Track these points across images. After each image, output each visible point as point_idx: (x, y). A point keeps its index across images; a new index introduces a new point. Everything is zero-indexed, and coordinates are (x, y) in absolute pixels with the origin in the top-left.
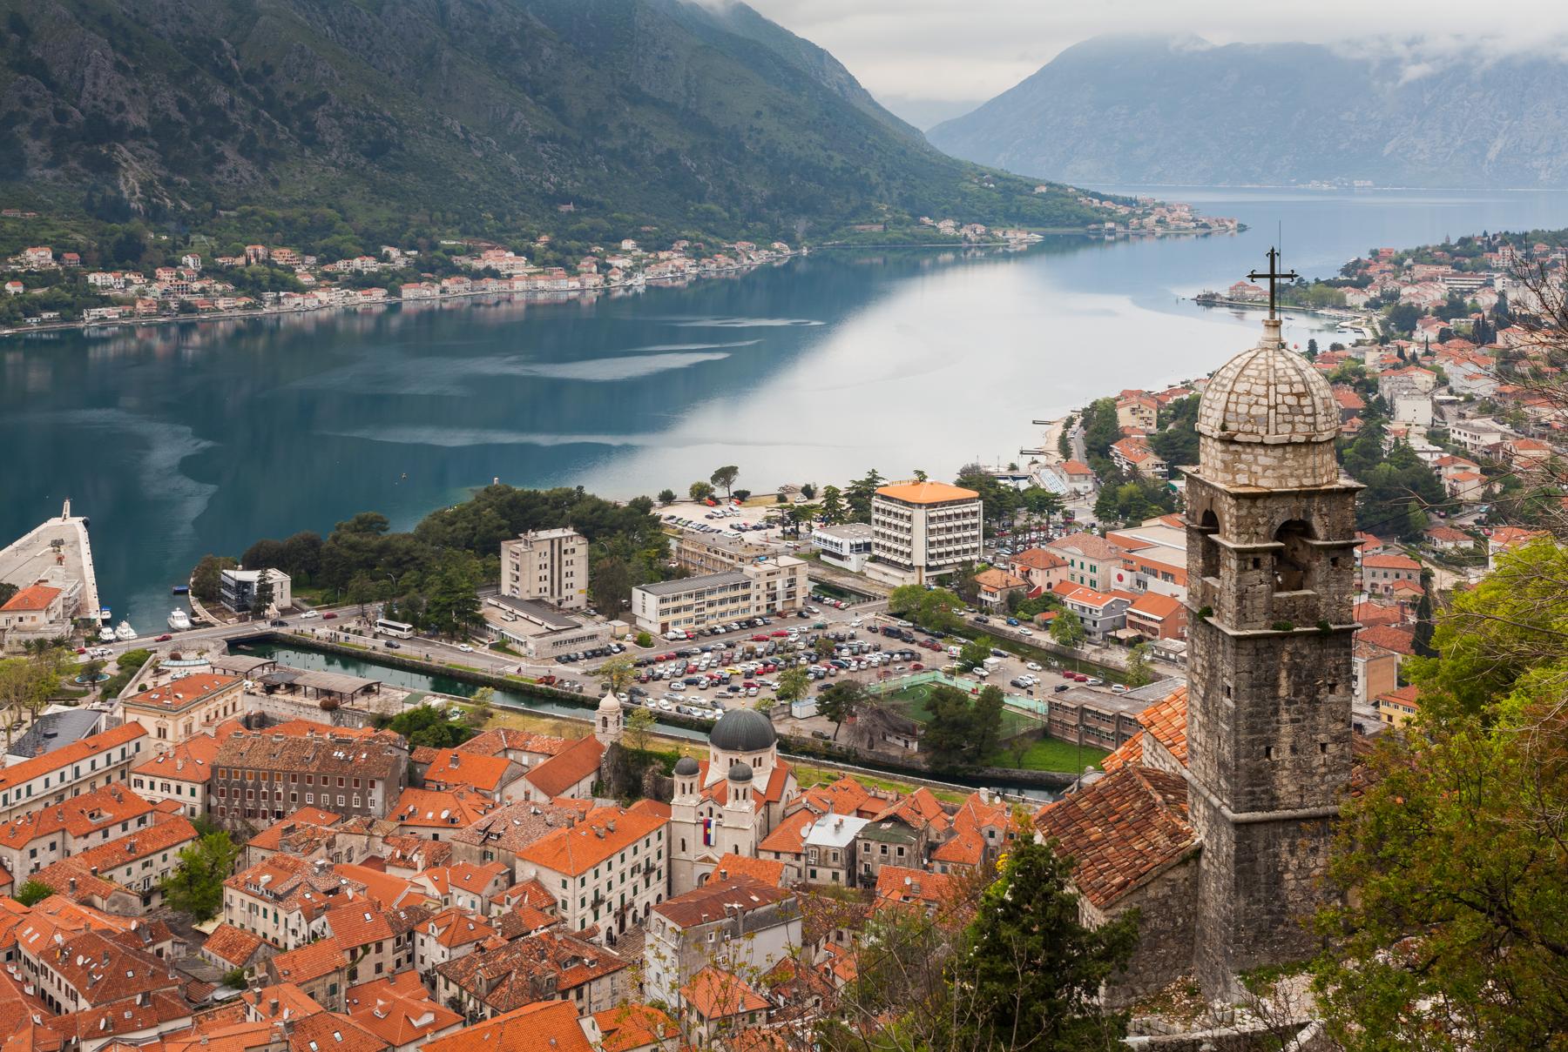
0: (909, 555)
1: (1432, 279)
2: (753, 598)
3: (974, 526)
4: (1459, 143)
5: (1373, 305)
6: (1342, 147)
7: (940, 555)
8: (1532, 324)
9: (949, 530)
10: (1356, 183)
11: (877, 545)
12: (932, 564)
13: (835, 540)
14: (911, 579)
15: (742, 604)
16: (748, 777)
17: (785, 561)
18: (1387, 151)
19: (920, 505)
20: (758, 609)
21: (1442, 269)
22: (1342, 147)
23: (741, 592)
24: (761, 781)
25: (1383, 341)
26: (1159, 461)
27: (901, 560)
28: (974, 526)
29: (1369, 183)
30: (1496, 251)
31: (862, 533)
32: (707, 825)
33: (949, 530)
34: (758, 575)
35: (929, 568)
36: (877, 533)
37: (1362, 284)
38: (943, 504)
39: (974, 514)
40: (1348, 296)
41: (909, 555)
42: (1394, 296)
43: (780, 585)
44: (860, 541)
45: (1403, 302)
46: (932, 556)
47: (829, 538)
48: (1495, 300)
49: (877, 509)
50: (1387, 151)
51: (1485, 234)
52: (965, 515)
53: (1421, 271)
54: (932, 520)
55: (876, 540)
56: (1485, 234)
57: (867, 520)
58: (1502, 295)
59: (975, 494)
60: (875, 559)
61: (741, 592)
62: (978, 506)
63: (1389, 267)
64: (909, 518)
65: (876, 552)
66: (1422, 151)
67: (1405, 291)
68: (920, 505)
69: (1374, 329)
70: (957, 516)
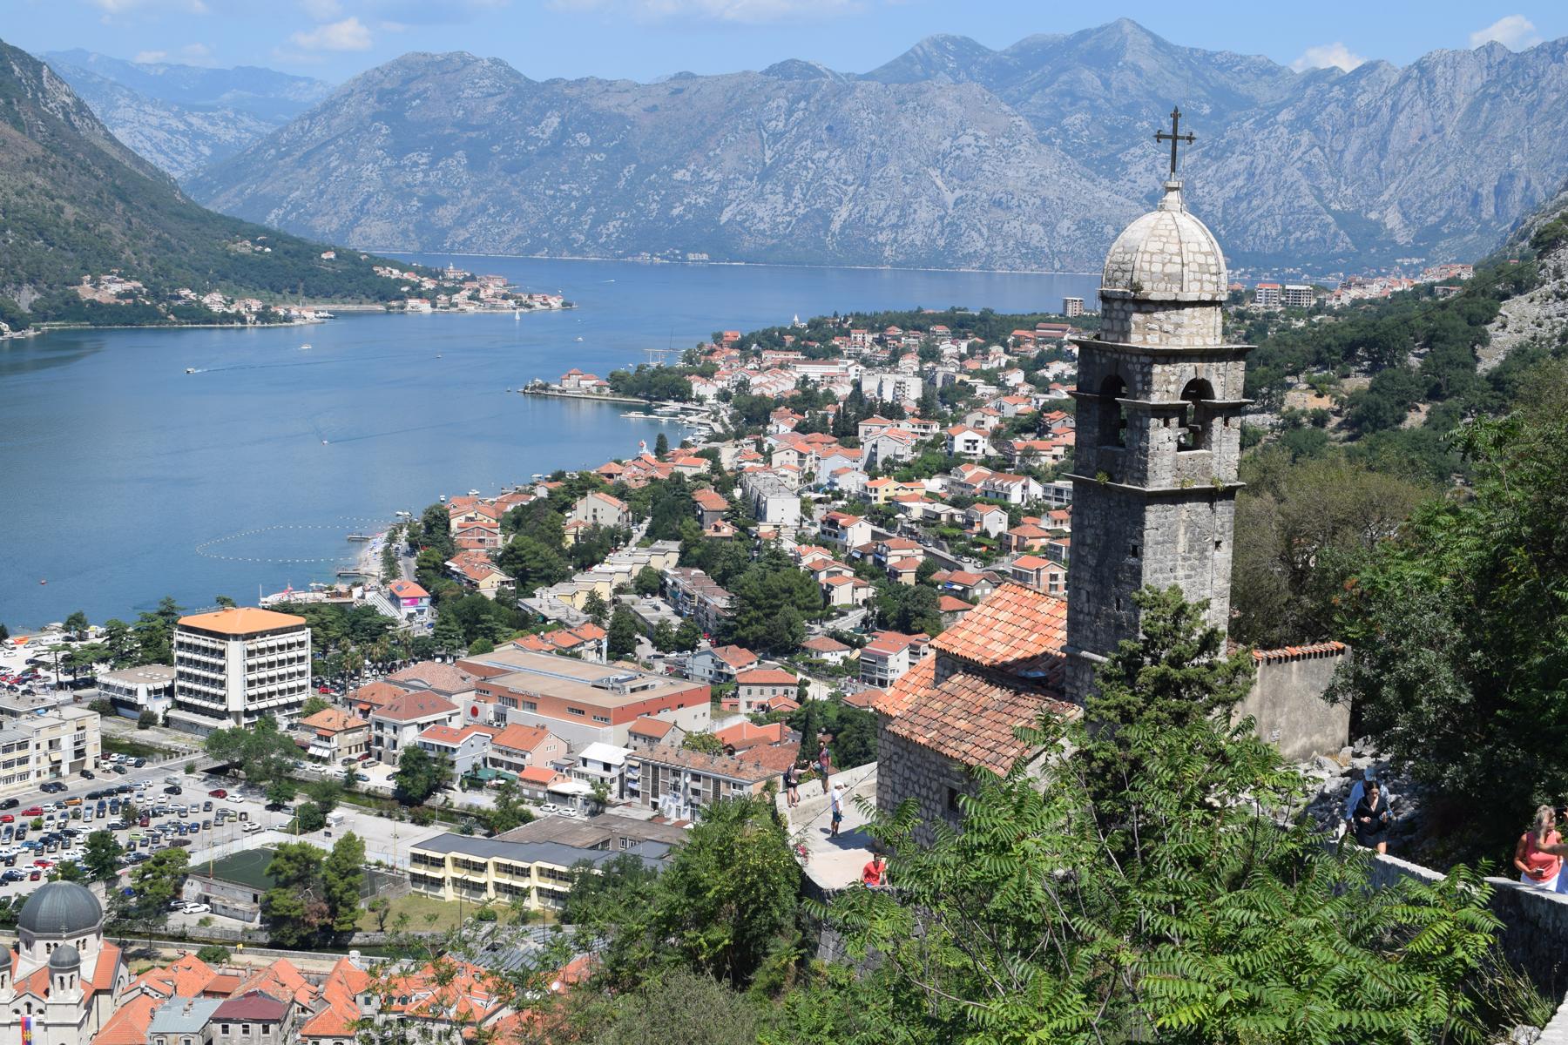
0: (222, 699)
1: (783, 366)
2: (32, 763)
3: (301, 659)
4: (801, 211)
5: (724, 396)
6: (675, 212)
7: (261, 696)
8: (893, 412)
9: (271, 665)
10: (691, 256)
11: (182, 689)
12: (252, 707)
13: (128, 686)
14: (226, 725)
15: (17, 769)
16: (75, 964)
17: (71, 712)
18: (724, 219)
19: (236, 637)
20: (39, 774)
21: (791, 356)
22: (675, 212)
23: (16, 754)
24: (88, 968)
25: (739, 436)
26: (505, 578)
27: (213, 706)
28: (301, 659)
29: (705, 257)
30: (848, 334)
31: (162, 676)
32: (26, 1025)
33: (271, 665)
34: (38, 731)
35: (247, 713)
36: (181, 675)
37: (708, 373)
38: (263, 634)
39: (301, 644)
40: (695, 387)
41: (222, 699)
42: (743, 385)
43: (67, 744)
44: (159, 686)
45: (756, 392)
46: (251, 698)
47: (120, 683)
48: (849, 390)
49: (181, 645)
50: (724, 219)
51: (836, 316)
52: (290, 646)
53: (770, 357)
54: (251, 653)
55: (181, 683)
56: (836, 316)
57: (166, 660)
58: (857, 385)
59: (301, 621)
60: (180, 705)
61: (16, 754)
62: (305, 635)
63: (735, 353)
64: (222, 654)
65: (180, 698)
66: (762, 219)
67: (755, 380)
68: (236, 637)
69: (724, 425)
70: (281, 648)
